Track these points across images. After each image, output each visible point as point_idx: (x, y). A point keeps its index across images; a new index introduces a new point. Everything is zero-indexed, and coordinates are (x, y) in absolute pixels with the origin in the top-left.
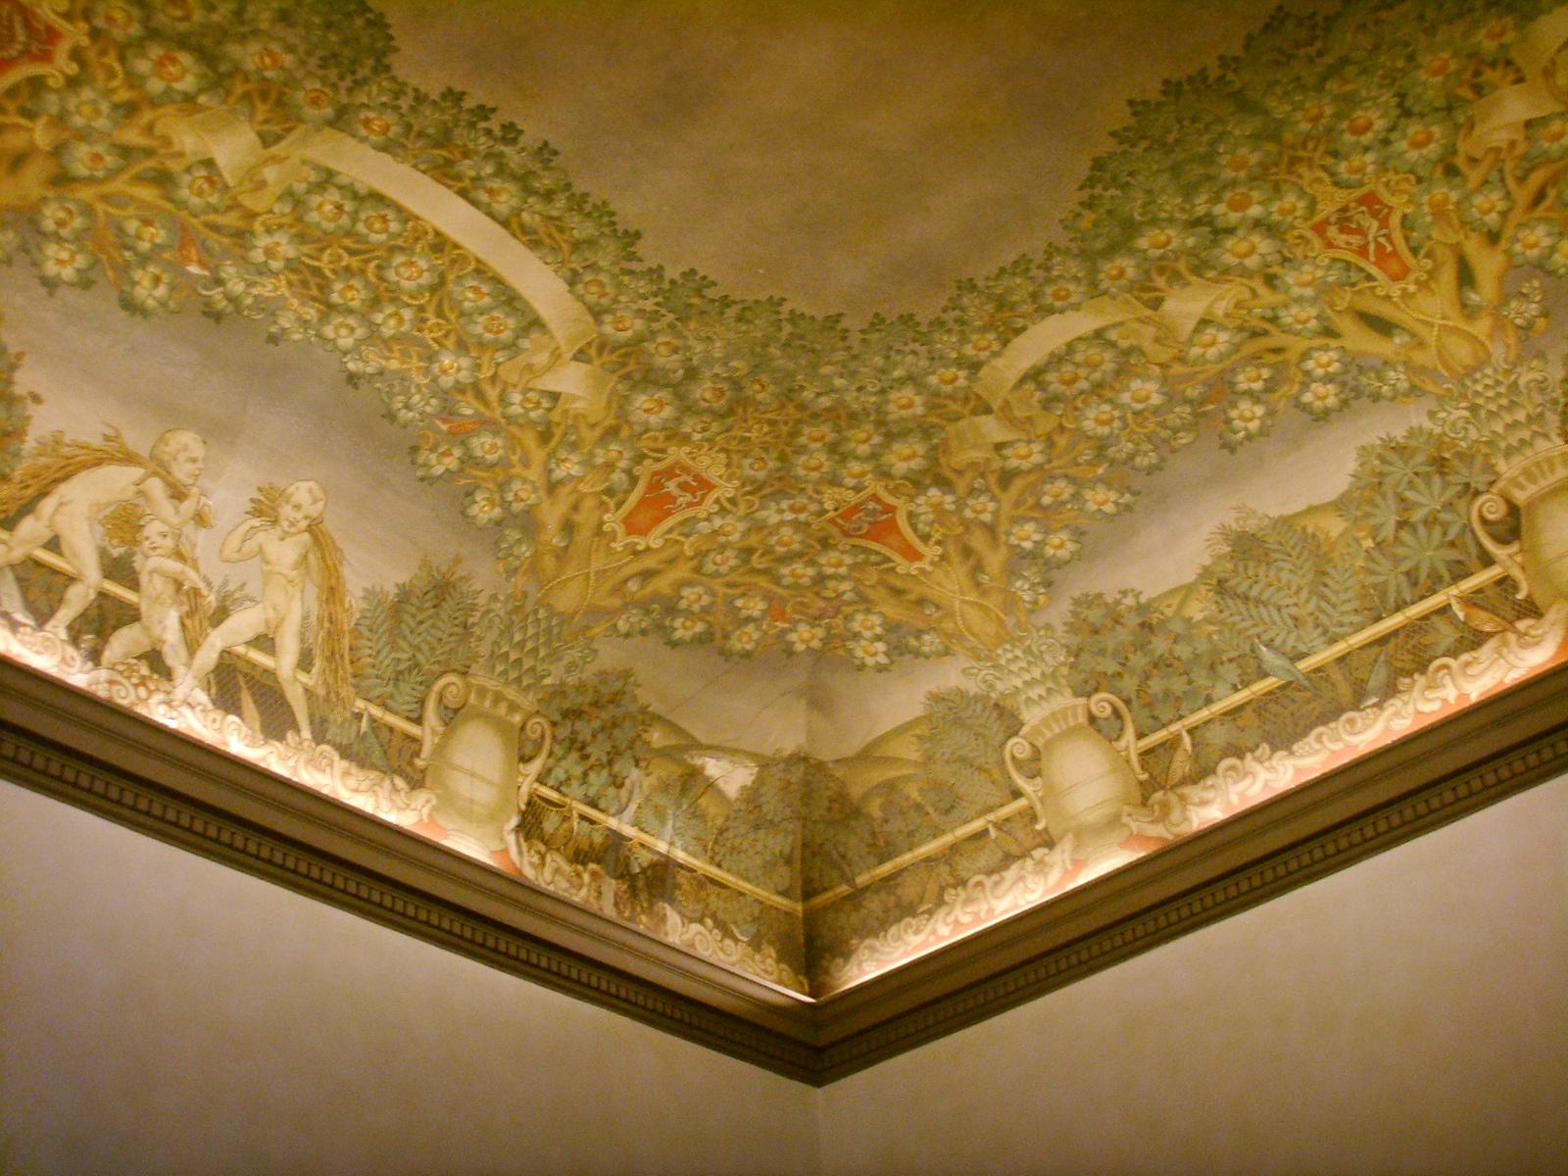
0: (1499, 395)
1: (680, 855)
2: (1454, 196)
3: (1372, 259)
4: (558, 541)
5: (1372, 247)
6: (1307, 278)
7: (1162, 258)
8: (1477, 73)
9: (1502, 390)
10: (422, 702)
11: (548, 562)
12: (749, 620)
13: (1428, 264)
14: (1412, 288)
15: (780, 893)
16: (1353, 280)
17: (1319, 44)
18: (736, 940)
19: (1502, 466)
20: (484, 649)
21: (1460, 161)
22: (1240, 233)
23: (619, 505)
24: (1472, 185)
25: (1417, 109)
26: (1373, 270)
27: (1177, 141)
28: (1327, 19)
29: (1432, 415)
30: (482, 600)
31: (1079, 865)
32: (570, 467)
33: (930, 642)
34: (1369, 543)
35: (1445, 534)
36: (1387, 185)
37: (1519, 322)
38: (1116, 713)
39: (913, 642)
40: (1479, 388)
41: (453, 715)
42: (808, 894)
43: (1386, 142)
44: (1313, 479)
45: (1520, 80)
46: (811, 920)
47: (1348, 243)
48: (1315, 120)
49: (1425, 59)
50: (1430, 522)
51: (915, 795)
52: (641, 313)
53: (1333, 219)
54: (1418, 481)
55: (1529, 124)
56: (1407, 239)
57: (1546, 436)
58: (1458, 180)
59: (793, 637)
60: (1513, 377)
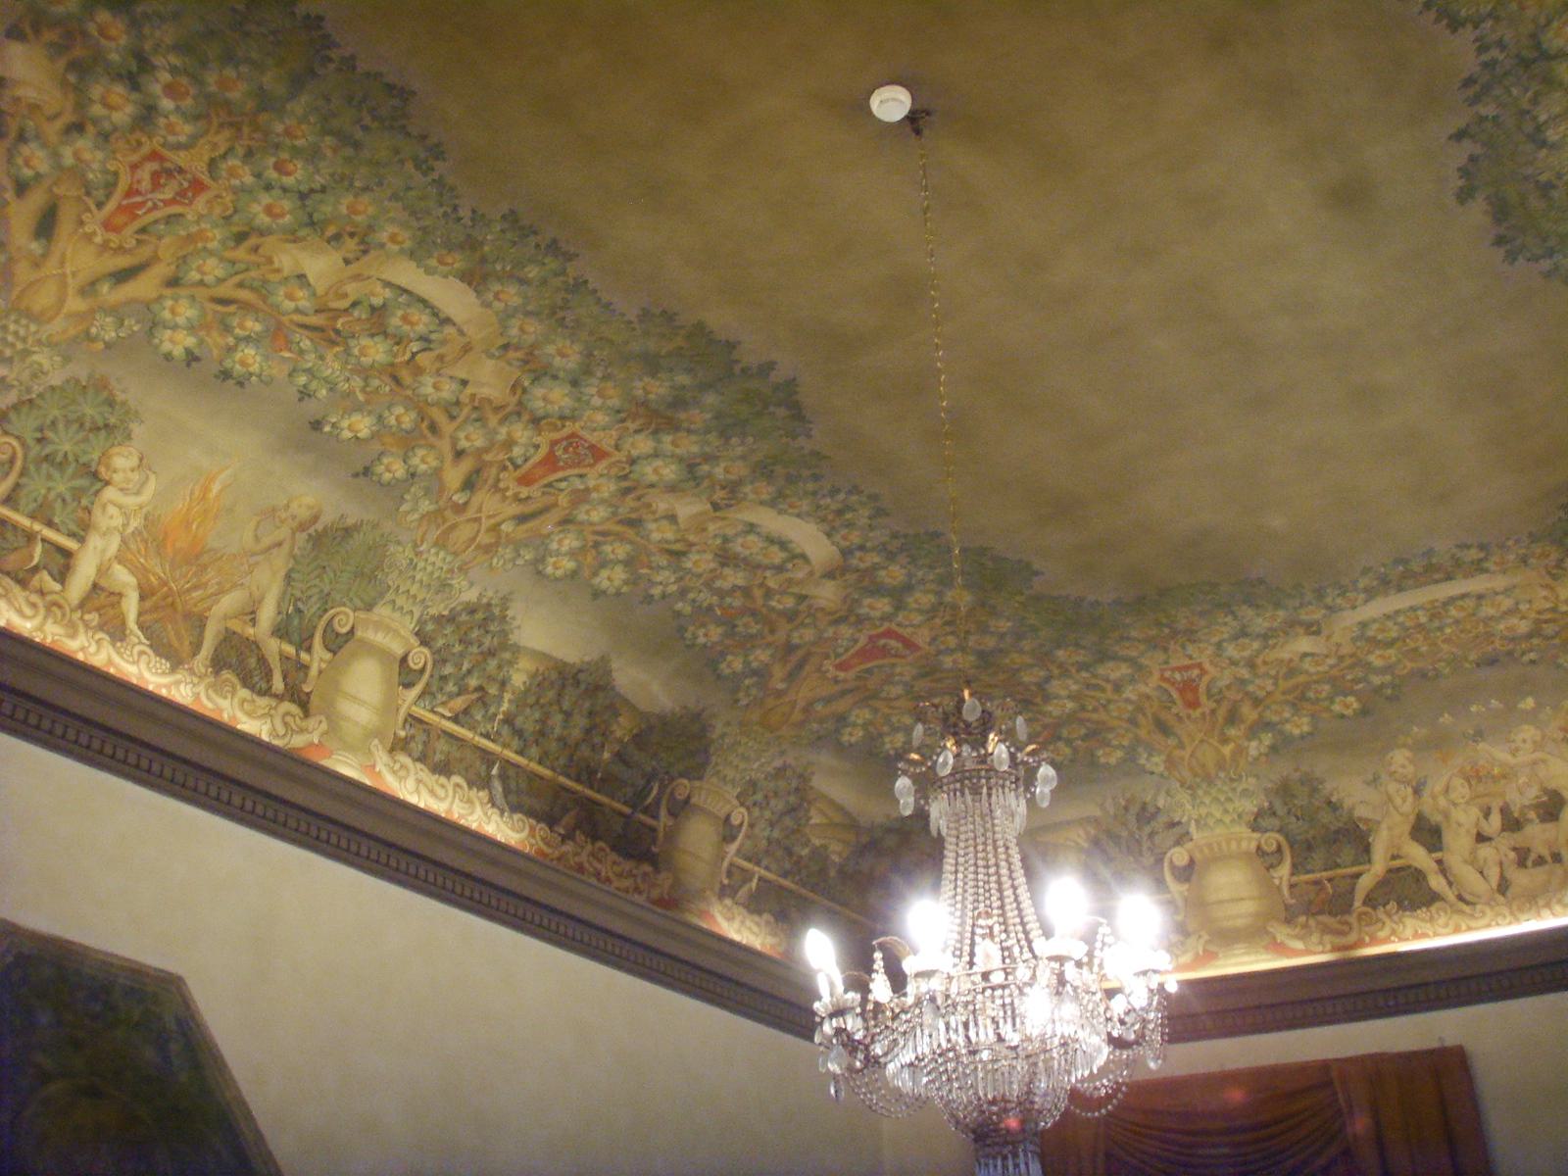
0: (13, 345)
2: (213, 245)
3: (125, 202)
5: (139, 199)
6: (87, 156)
7: (85, 34)
8: (352, 235)
9: (20, 346)
13: (131, 243)
14: (98, 239)
16: (95, 193)
17: (376, 125)
21: (253, 241)
22: (135, 96)
24: (228, 254)
25: (308, 202)
26: (111, 206)
27: (247, 34)
28: (404, 127)
36: (218, 196)
37: (94, 330)
40: (12, 327)
43: (268, 187)
45: (347, 262)
47: (139, 182)
48: (288, 133)
49: (366, 198)
53: (168, 165)
55: (302, 277)
56: (156, 222)
58: (232, 244)
60: (36, 349)
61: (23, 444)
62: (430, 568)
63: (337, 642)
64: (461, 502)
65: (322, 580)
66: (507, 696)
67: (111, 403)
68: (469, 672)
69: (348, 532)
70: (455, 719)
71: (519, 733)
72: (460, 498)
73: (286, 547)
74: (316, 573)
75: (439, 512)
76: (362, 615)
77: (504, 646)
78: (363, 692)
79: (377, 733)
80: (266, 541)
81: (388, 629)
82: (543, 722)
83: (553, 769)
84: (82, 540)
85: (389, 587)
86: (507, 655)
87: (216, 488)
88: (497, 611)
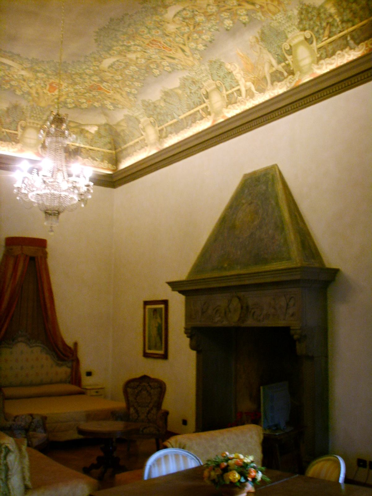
1: (82, 146)
4: (36, 95)
10: (17, 127)
11: (36, 99)
12: (83, 103)
15: (109, 150)
18: (96, 161)
19: (204, 83)
20: (28, 115)
23: (45, 89)
29: (189, 73)
30: (25, 107)
31: (150, 151)
32: (32, 84)
33: (119, 106)
34: (186, 96)
35: (198, 95)
38: (155, 122)
39: (116, 106)
41: (24, 128)
42: (115, 149)
44: (174, 82)
46: (116, 154)
50: (195, 93)
51: (127, 133)
52: (29, 63)
54: (191, 85)
57: (210, 79)
59: (94, 104)
61: (219, 80)
62: (282, 19)
63: (290, 52)
64: (259, 6)
65: (274, 45)
66: (336, 17)
67: (215, 62)
68: (321, 23)
69: (263, 33)
70: (329, 37)
71: (348, 21)
72: (258, 7)
73: (262, 48)
74: (271, 45)
75: (262, 12)
76: (288, 41)
77: (319, 9)
78: (304, 55)
79: (313, 62)
80: (258, 50)
81: (295, 37)
82: (351, 11)
83: (367, 18)
84: (238, 85)
85: (284, 31)
86: (322, 10)
87: (241, 54)
88: (304, 7)
